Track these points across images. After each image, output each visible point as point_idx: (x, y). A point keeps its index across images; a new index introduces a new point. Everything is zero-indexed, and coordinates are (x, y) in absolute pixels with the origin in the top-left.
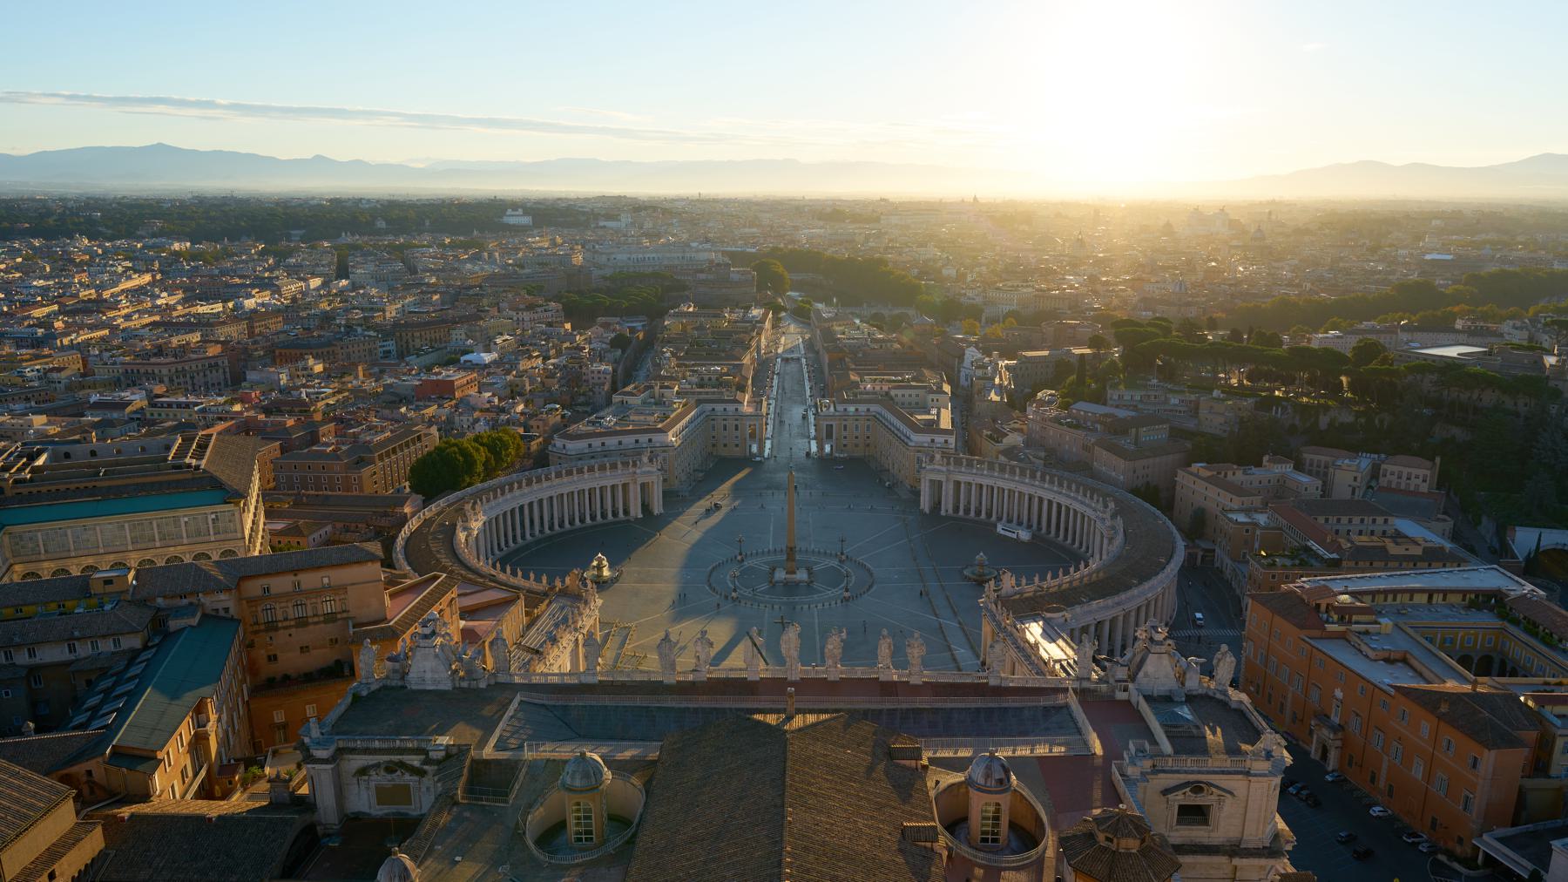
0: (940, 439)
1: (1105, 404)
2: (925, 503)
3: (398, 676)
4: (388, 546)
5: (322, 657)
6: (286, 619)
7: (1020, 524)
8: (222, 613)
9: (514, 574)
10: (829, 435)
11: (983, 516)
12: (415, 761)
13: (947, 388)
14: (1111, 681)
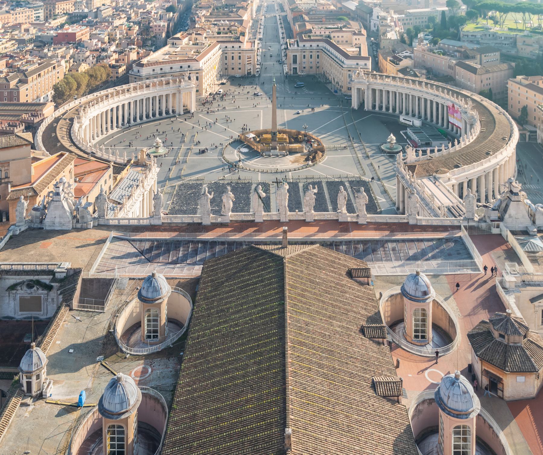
2: (355, 104)
10: (295, 61)
11: (391, 111)
14: (488, 221)
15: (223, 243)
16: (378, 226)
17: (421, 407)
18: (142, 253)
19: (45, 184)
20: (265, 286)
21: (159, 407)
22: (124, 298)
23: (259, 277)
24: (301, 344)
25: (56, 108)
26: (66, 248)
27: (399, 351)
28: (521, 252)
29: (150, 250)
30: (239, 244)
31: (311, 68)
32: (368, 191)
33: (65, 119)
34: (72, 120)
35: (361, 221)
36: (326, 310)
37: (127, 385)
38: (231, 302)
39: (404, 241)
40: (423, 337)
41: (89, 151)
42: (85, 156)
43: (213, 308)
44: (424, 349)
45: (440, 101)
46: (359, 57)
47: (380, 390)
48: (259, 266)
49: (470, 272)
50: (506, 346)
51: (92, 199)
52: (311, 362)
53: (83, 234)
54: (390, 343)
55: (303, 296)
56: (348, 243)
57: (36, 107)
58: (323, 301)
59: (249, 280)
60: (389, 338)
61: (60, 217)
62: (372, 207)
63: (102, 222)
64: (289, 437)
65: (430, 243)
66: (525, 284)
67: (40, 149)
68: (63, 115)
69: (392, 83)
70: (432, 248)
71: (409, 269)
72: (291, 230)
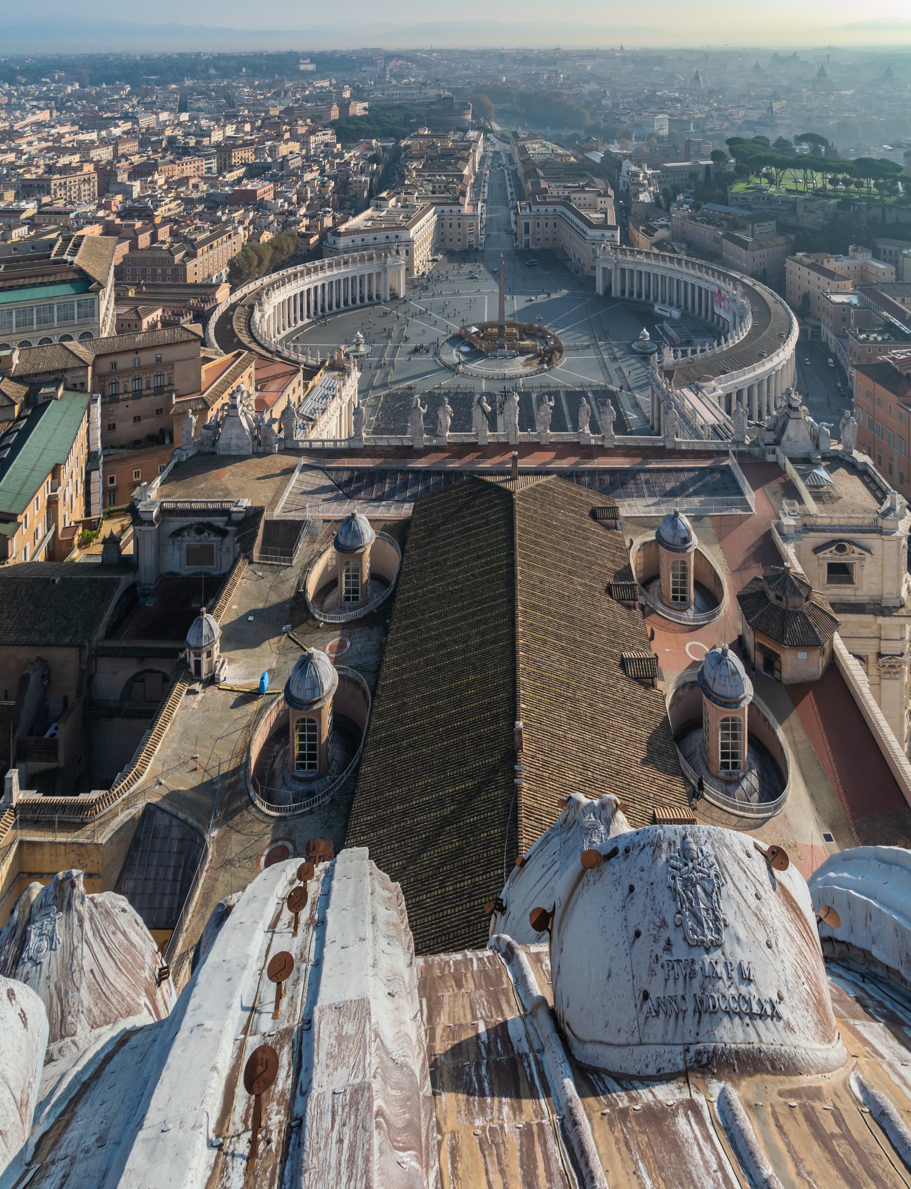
0: (608, 233)
4: (205, 328)
6: (126, 392)
12: (219, 521)
15: (439, 473)
16: (626, 451)
17: (680, 693)
18: (339, 486)
19: (218, 394)
20: (490, 530)
22: (316, 546)
23: (482, 518)
24: (535, 607)
25: (232, 291)
26: (244, 479)
27: (653, 617)
28: (801, 485)
29: (349, 482)
30: (458, 473)
32: (616, 404)
33: (243, 306)
34: (252, 307)
35: (608, 444)
36: (565, 562)
37: (320, 664)
38: (448, 552)
39: (659, 470)
40: (683, 599)
41: (273, 349)
42: (267, 356)
43: (426, 560)
44: (684, 615)
45: (704, 285)
46: (604, 226)
47: (631, 670)
48: (483, 504)
49: (739, 512)
50: (784, 611)
51: (277, 414)
52: (546, 632)
53: (266, 461)
54: (642, 607)
55: (537, 544)
56: (592, 472)
57: (207, 289)
58: (561, 551)
59: (470, 522)
60: (641, 600)
61: (238, 438)
62: (621, 426)
63: (289, 445)
64: (520, 732)
65: (692, 474)
66: (807, 528)
67: (212, 347)
68: (241, 300)
69: (645, 260)
70: (694, 481)
71: (665, 510)
72: (522, 456)
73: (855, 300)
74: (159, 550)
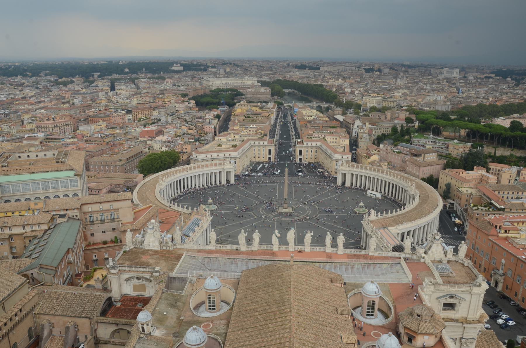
1: (411, 144)
2: (339, 182)
3: (140, 244)
5: (109, 236)
7: (377, 191)
8: (75, 217)
9: (178, 205)
13: (348, 136)
21: (217, 343)
31: (311, 158)
73: (474, 191)
74: (120, 285)
